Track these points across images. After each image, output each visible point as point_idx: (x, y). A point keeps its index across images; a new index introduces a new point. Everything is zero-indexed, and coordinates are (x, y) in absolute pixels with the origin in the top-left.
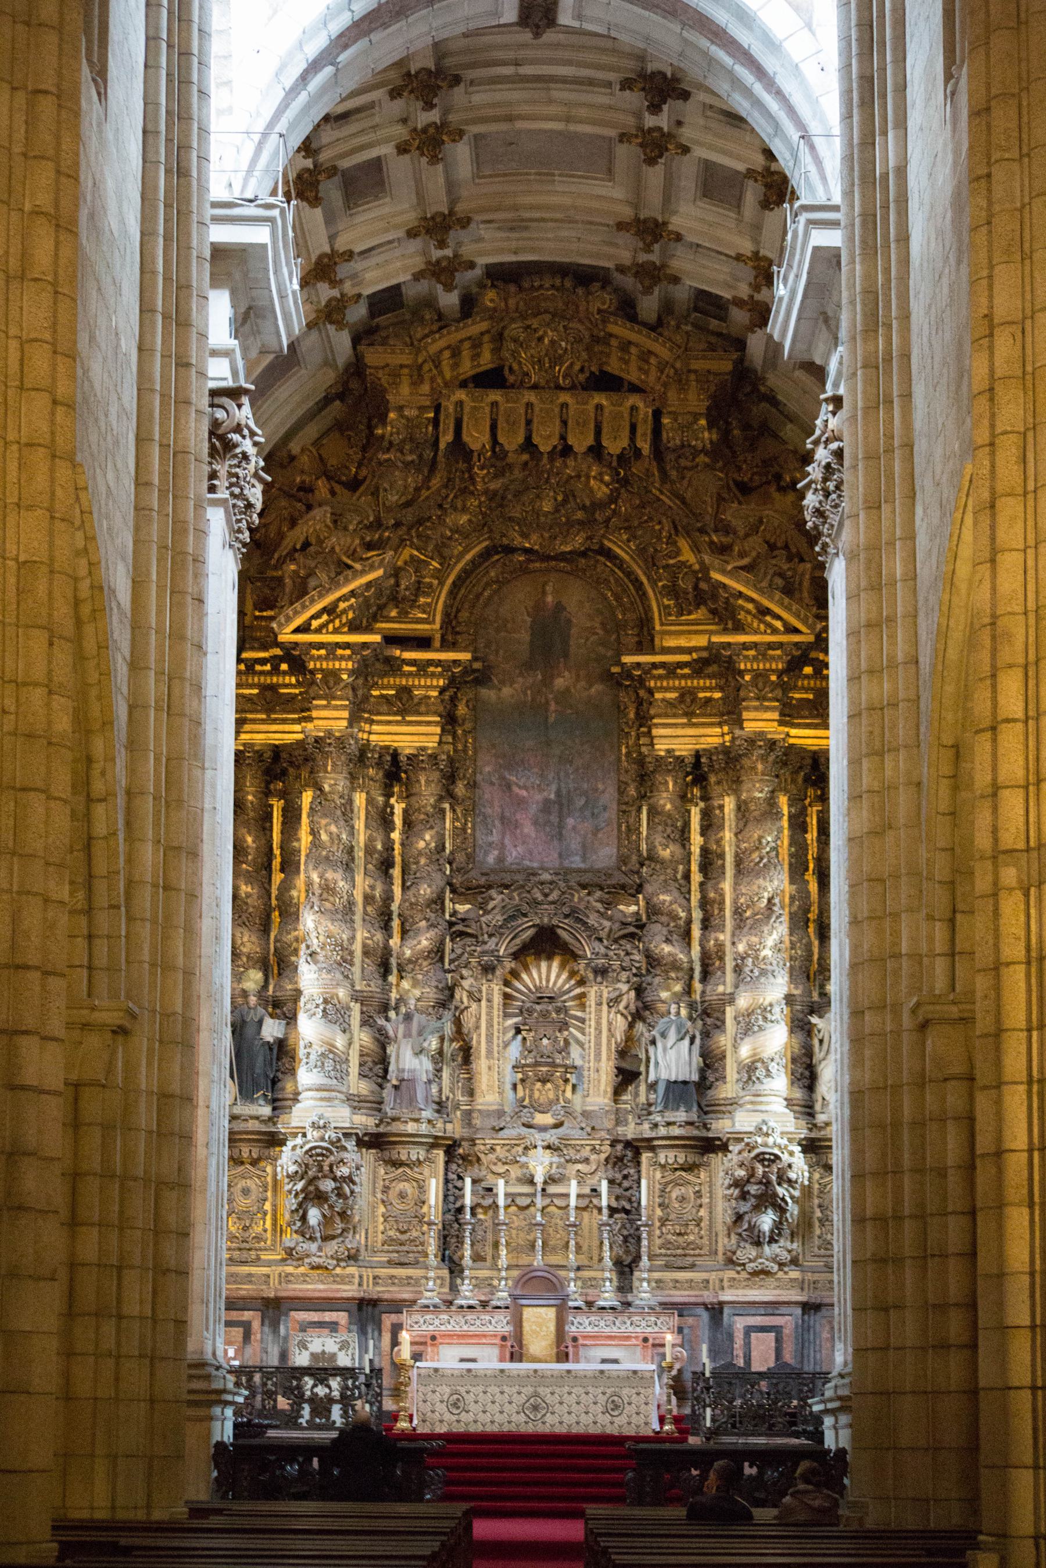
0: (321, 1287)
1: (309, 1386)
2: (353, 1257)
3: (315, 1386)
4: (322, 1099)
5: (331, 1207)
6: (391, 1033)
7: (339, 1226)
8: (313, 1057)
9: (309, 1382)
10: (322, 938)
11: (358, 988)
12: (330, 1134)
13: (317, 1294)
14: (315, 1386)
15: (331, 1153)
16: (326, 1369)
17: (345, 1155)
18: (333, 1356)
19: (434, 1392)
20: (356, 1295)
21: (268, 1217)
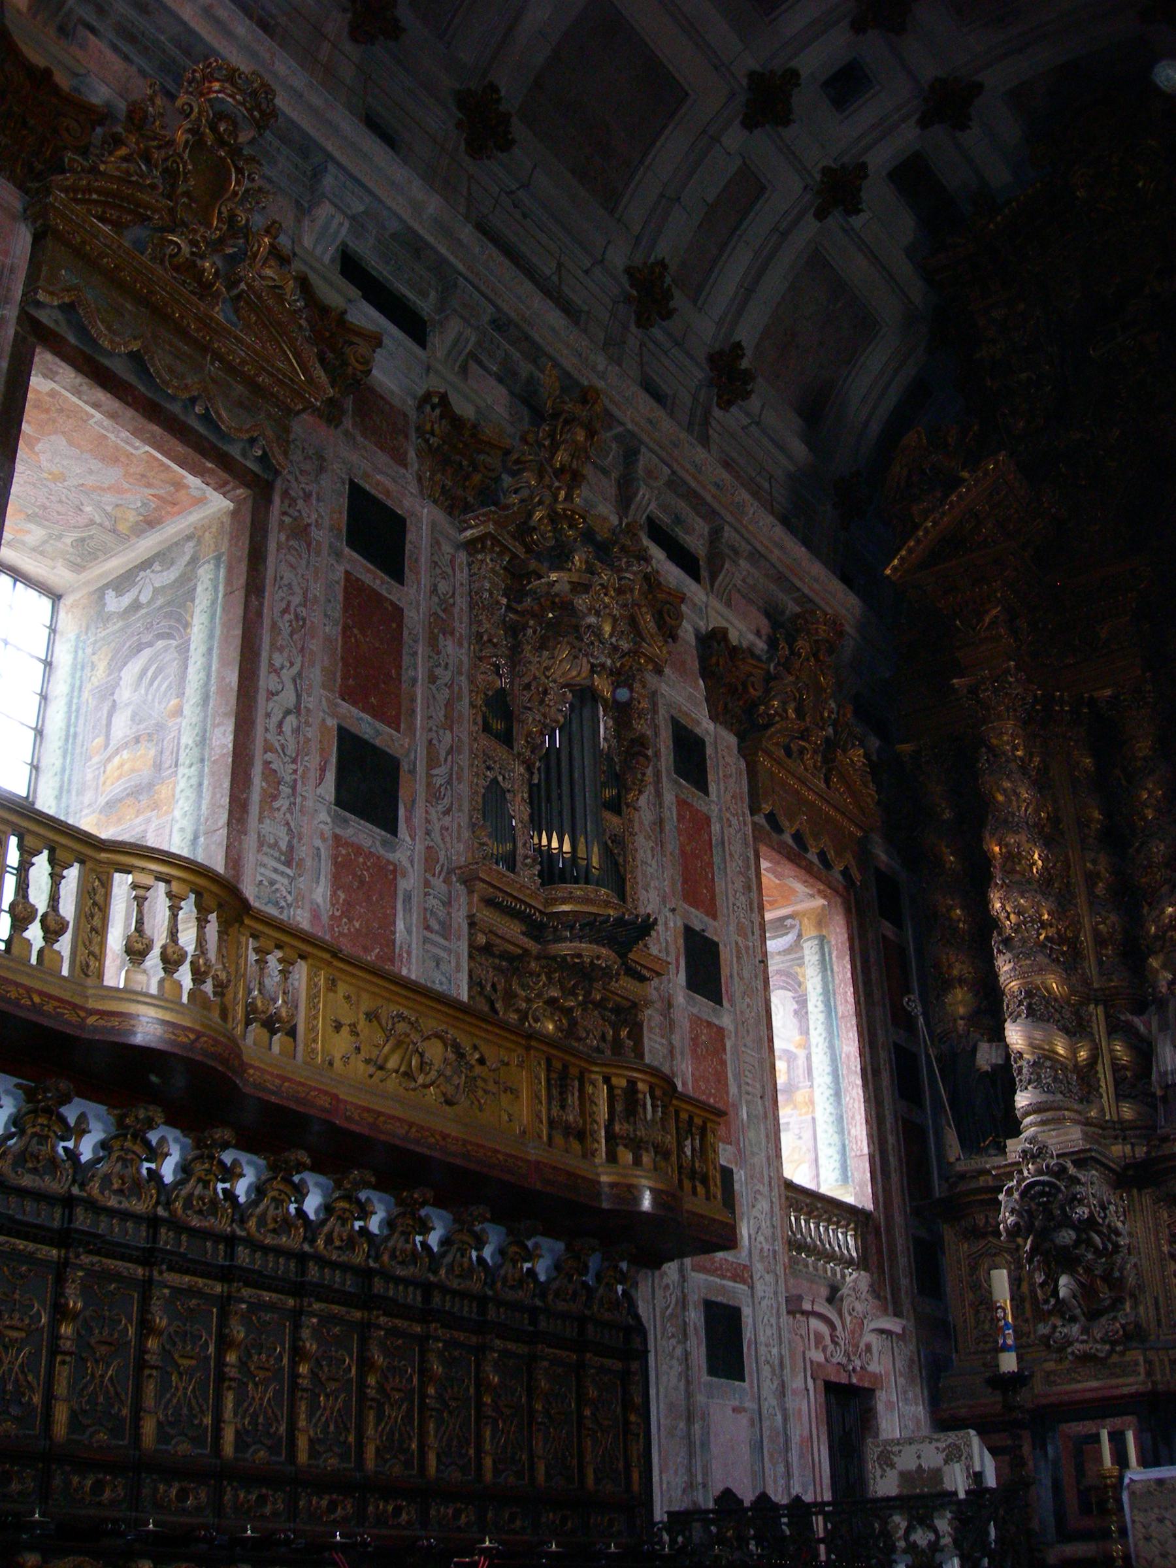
0: (1094, 1384)
1: (901, 1532)
2: (1134, 1335)
3: (909, 1530)
4: (1043, 1123)
5: (1088, 1270)
6: (1142, 1028)
7: (1105, 1293)
8: (1025, 1071)
9: (899, 1521)
10: (1012, 916)
11: (1096, 985)
12: (1053, 1162)
13: (1088, 1395)
14: (909, 1530)
15: (1059, 1189)
16: (921, 1497)
17: (1078, 1188)
18: (936, 1475)
19: (1161, 1520)
20: (1142, 1388)
21: (1027, 1305)
